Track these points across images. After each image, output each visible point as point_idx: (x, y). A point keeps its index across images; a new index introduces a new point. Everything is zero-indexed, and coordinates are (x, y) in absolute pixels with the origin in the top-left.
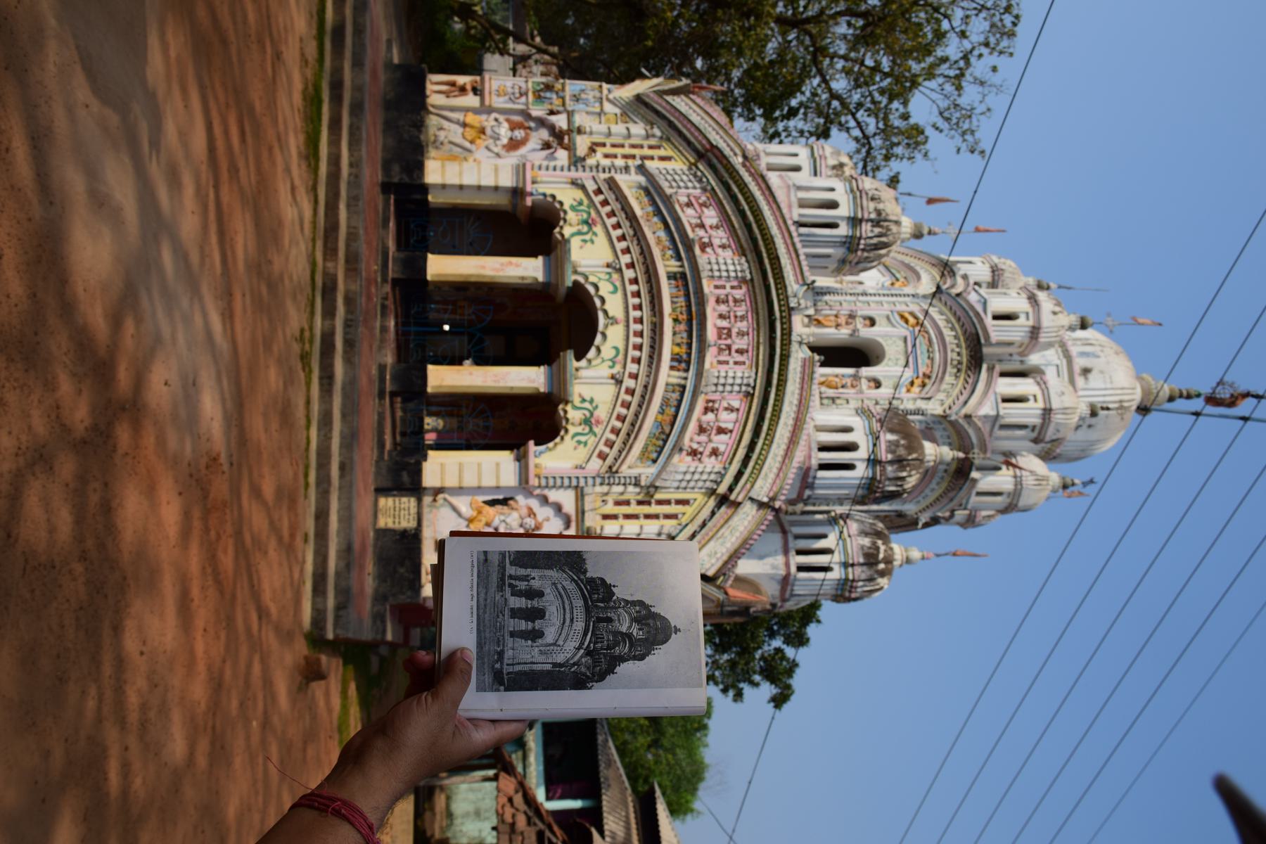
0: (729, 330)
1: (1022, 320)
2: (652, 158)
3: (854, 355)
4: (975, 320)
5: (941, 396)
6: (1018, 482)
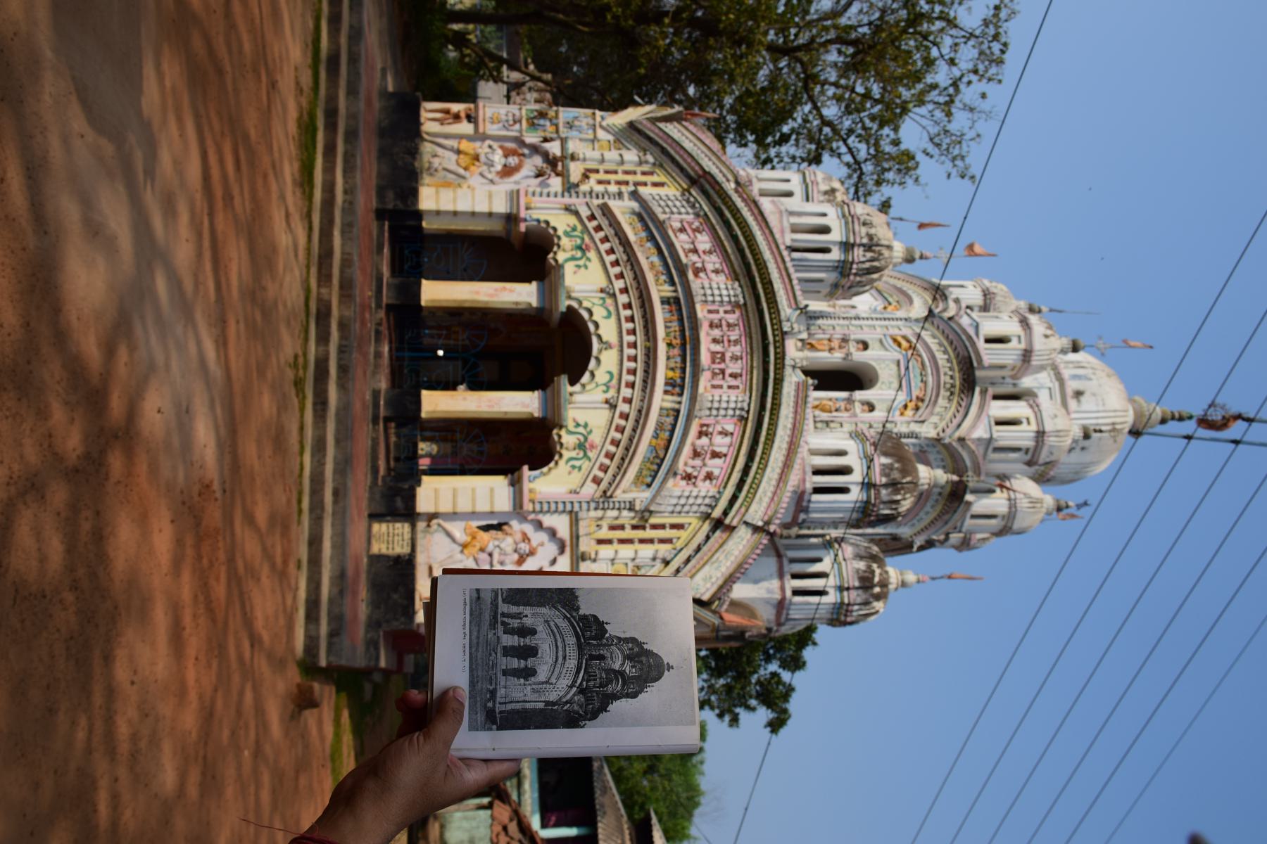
0: (723, 354)
1: (1014, 343)
2: (645, 184)
3: (848, 379)
4: (967, 344)
5: (935, 419)
6: (1012, 504)
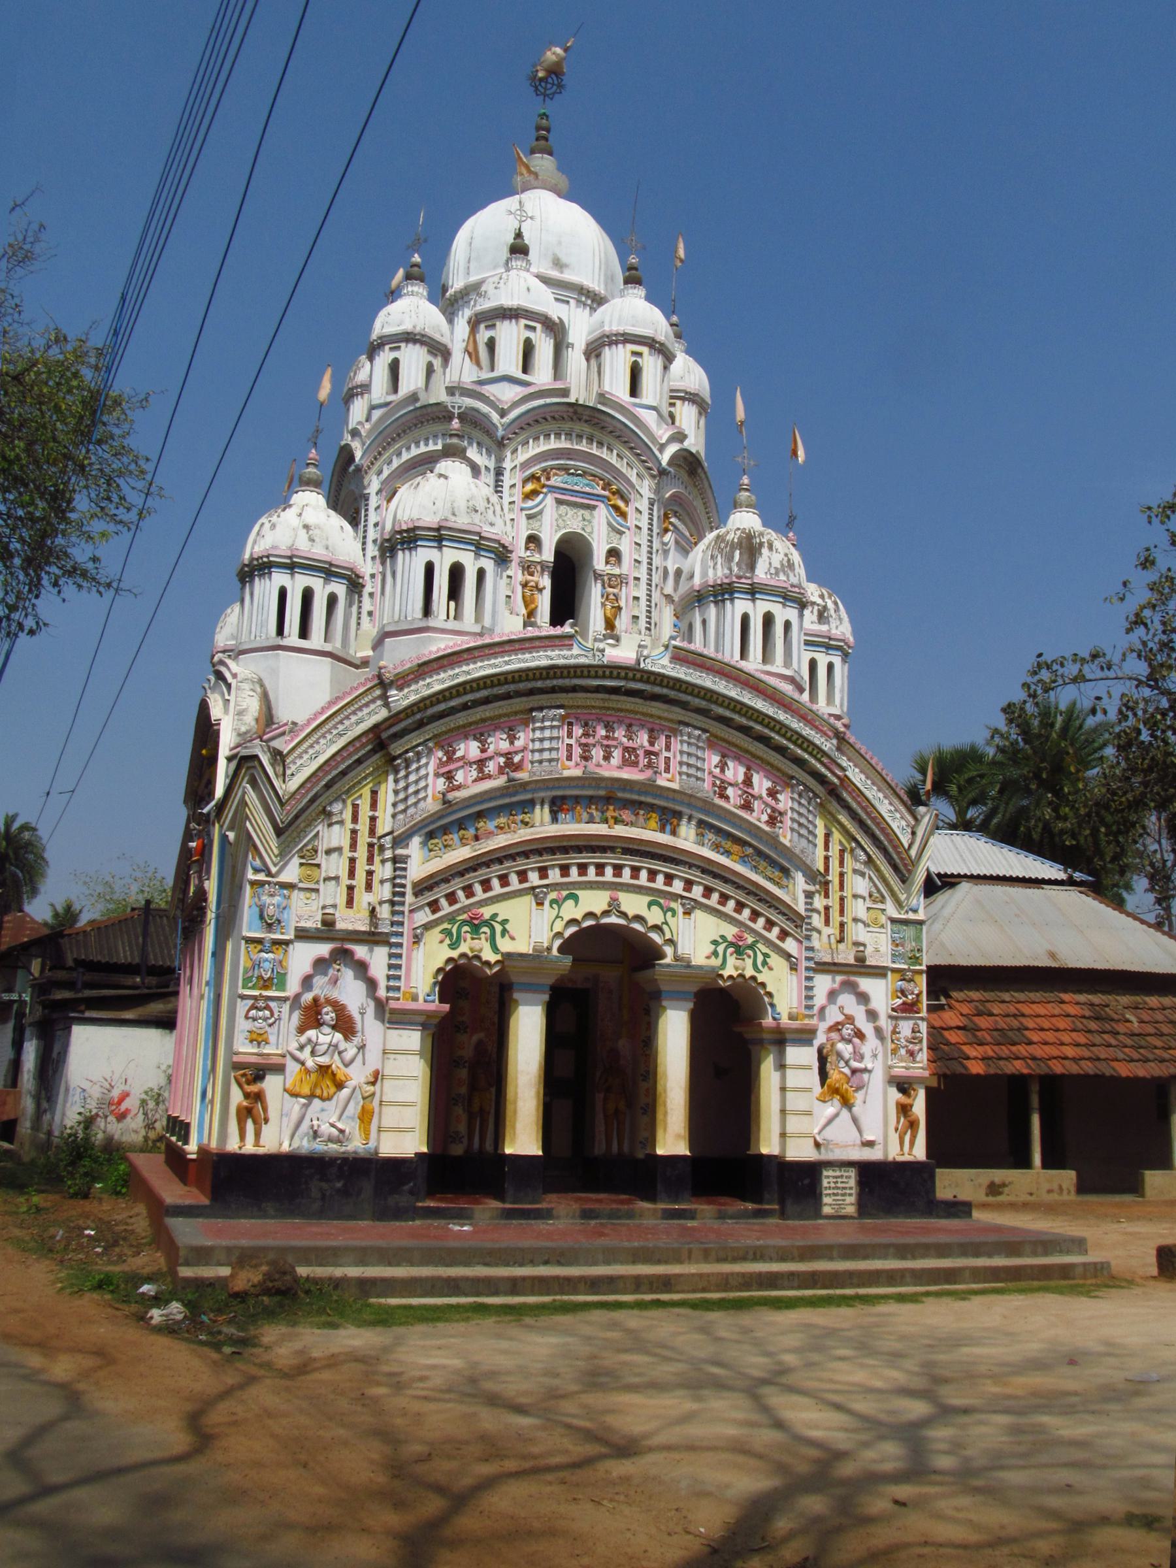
0: (626, 749)
2: (373, 819)
3: (568, 572)
